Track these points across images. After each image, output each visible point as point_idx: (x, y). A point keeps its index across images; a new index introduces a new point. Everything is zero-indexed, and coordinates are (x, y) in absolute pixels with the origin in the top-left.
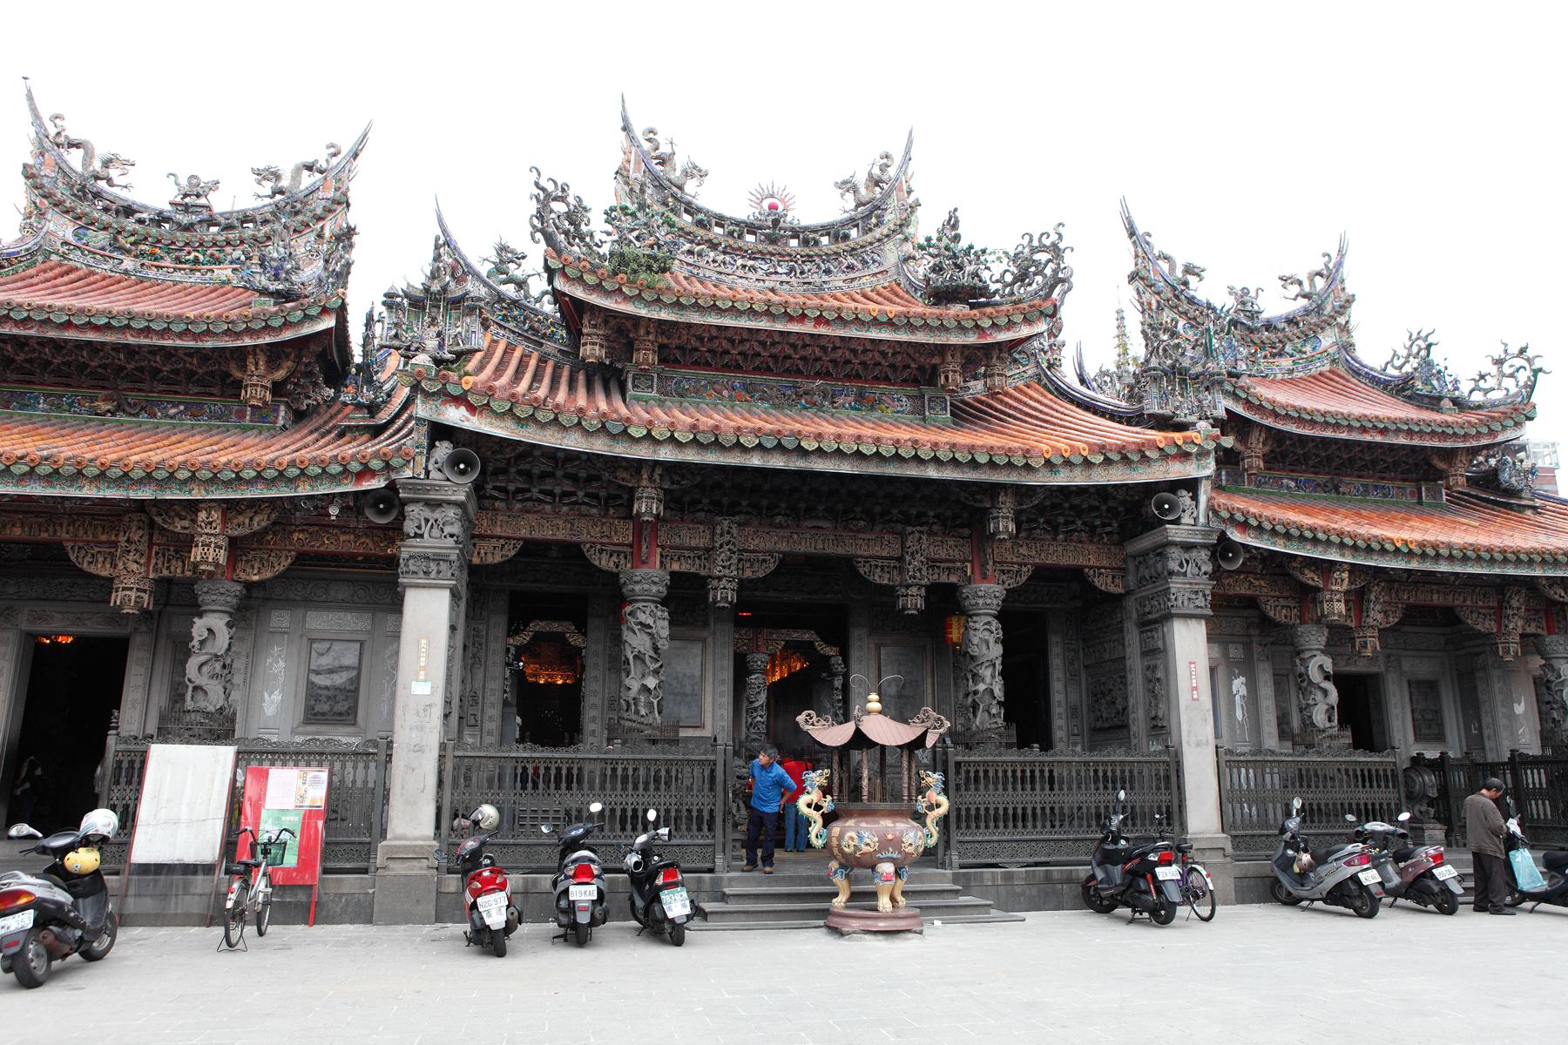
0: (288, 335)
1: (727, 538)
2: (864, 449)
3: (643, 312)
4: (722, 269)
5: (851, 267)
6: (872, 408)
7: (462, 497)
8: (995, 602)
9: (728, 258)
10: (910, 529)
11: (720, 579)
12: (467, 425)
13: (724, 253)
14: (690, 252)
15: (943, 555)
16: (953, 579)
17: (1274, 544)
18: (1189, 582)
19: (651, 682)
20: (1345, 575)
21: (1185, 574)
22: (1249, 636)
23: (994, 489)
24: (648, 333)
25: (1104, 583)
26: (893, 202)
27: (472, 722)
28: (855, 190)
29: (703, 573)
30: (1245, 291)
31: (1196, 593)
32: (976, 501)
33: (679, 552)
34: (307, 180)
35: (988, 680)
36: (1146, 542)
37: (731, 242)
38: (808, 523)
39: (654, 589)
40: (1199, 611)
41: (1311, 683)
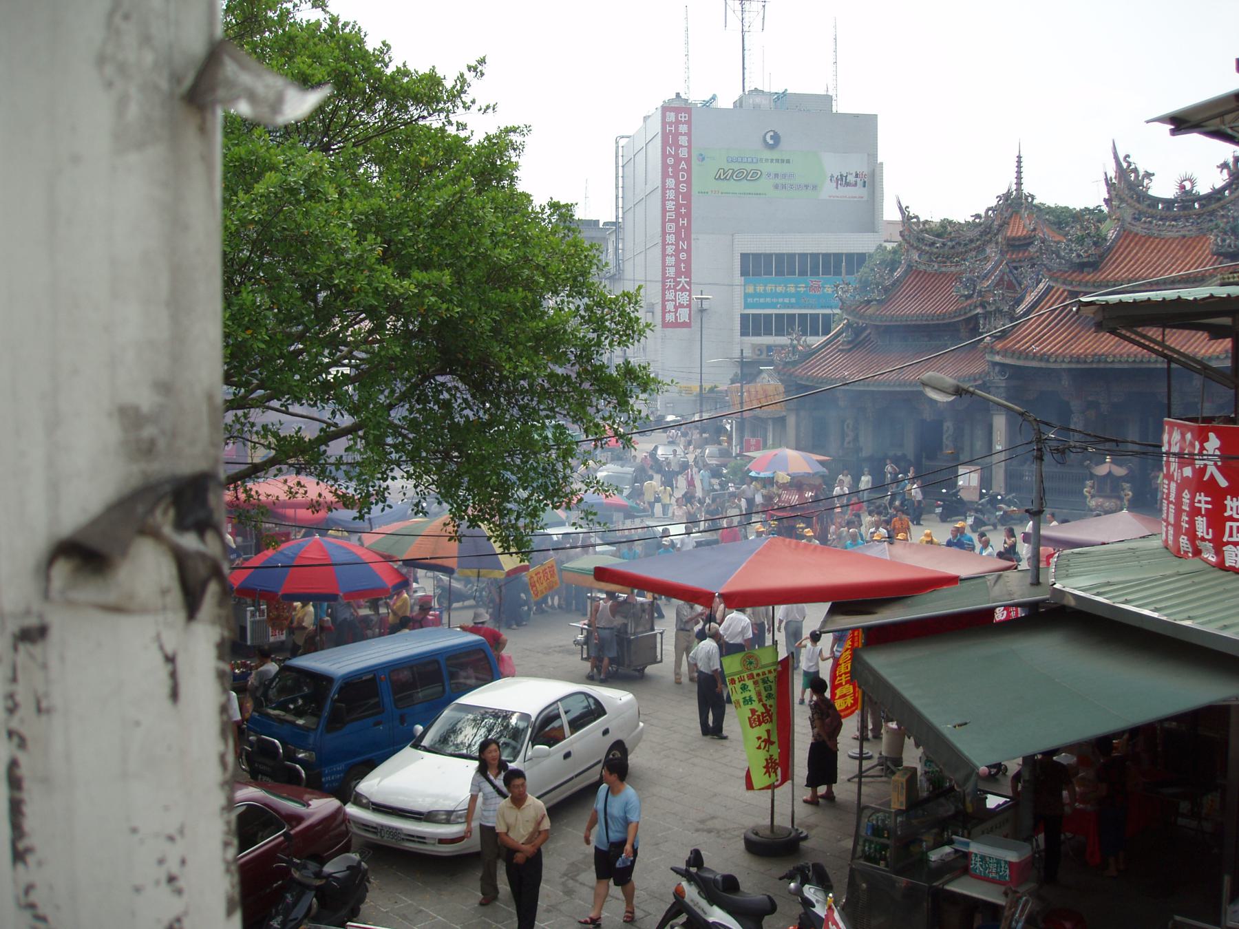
0: (969, 315)
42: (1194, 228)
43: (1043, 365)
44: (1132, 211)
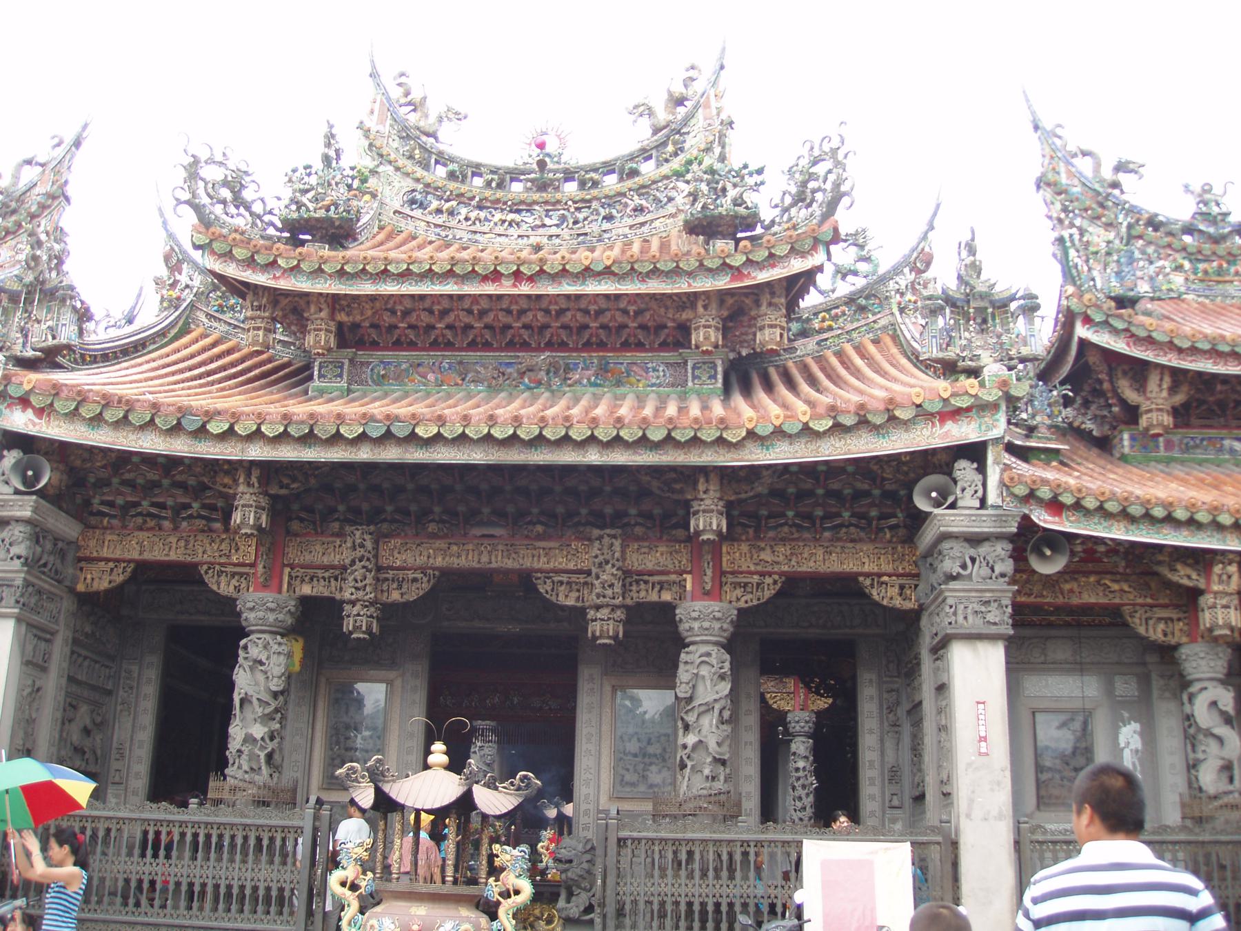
1: (360, 552)
2: (498, 433)
3: (303, 285)
4: (478, 227)
5: (639, 210)
6: (619, 383)
7: (27, 513)
8: (717, 625)
9: (482, 214)
10: (596, 532)
11: (353, 603)
12: (32, 430)
13: (480, 207)
14: (439, 211)
15: (650, 566)
16: (667, 596)
17: (1109, 528)
18: (975, 592)
19: (258, 731)
20: (1233, 569)
21: (970, 577)
22: (1144, 664)
23: (693, 474)
24: (321, 310)
25: (888, 596)
26: (699, 121)
27: (117, 779)
28: (651, 113)
29: (338, 596)
30: (1207, 189)
31: (987, 603)
32: (673, 491)
33: (312, 572)
34: (29, 174)
35: (704, 732)
36: (928, 536)
37: (488, 193)
38: (478, 531)
39: (271, 617)
40: (993, 630)
41: (1199, 729)
42: (565, 233)
43: (181, 447)
44: (408, 184)
